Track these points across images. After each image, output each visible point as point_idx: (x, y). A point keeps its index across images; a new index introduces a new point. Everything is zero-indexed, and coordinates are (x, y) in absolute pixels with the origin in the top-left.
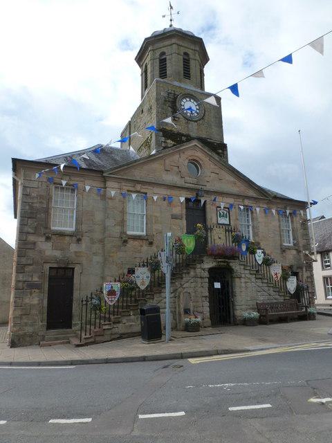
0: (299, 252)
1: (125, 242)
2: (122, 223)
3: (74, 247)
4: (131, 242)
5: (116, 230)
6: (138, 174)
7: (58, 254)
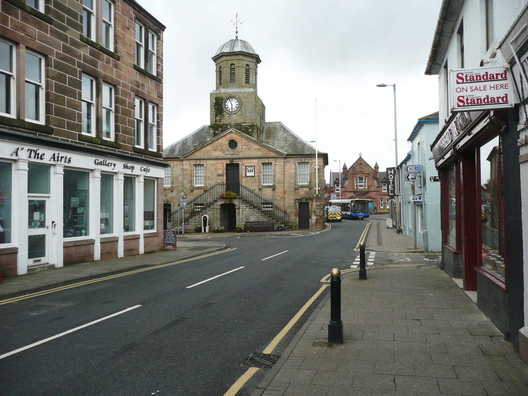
1: (192, 191)
2: (191, 181)
3: (170, 195)
4: (195, 190)
5: (188, 186)
6: (198, 155)
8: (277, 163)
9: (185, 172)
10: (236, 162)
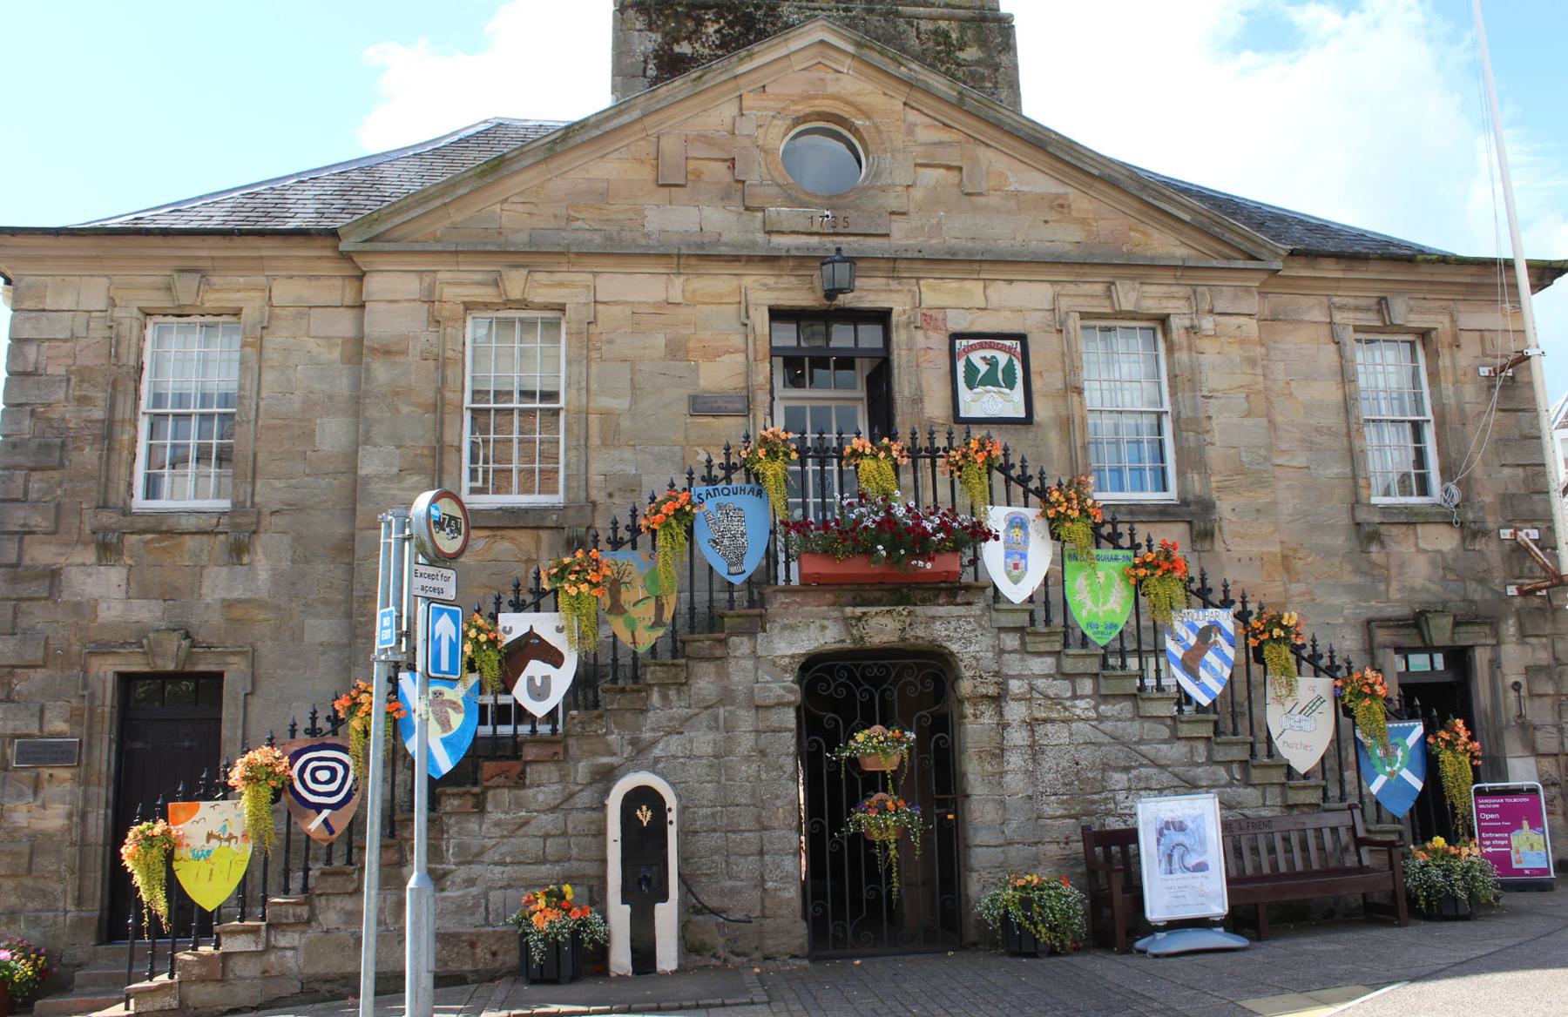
0: (1472, 532)
3: (219, 585)
7: (147, 612)
8: (1207, 323)
9: (381, 372)
10: (869, 293)
